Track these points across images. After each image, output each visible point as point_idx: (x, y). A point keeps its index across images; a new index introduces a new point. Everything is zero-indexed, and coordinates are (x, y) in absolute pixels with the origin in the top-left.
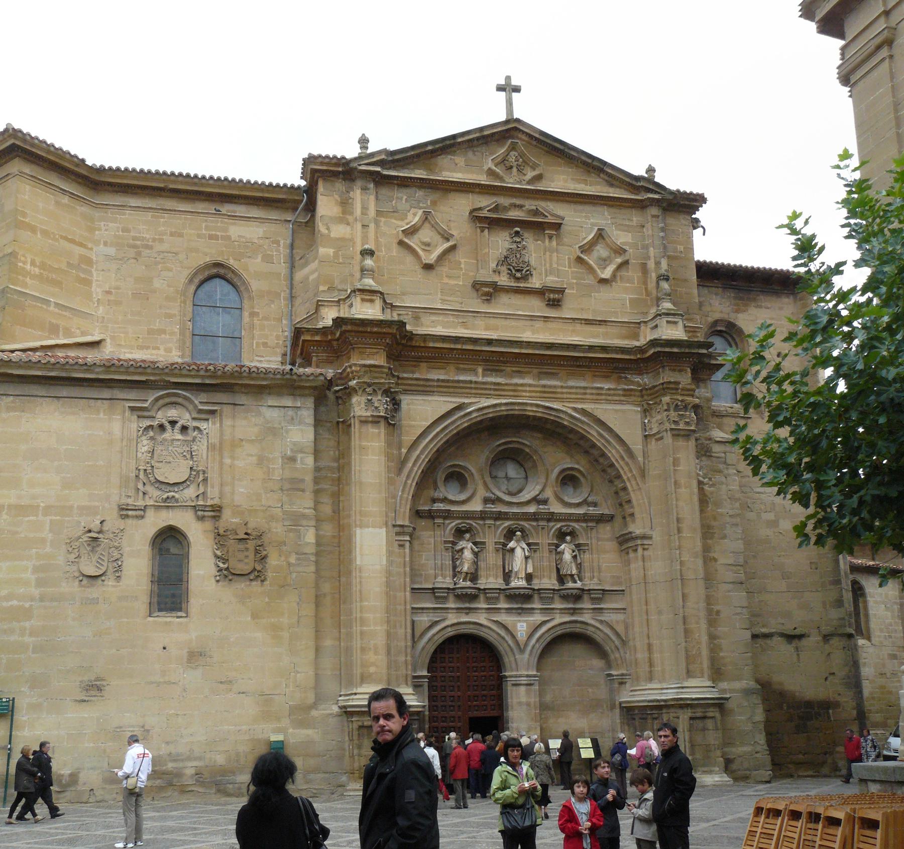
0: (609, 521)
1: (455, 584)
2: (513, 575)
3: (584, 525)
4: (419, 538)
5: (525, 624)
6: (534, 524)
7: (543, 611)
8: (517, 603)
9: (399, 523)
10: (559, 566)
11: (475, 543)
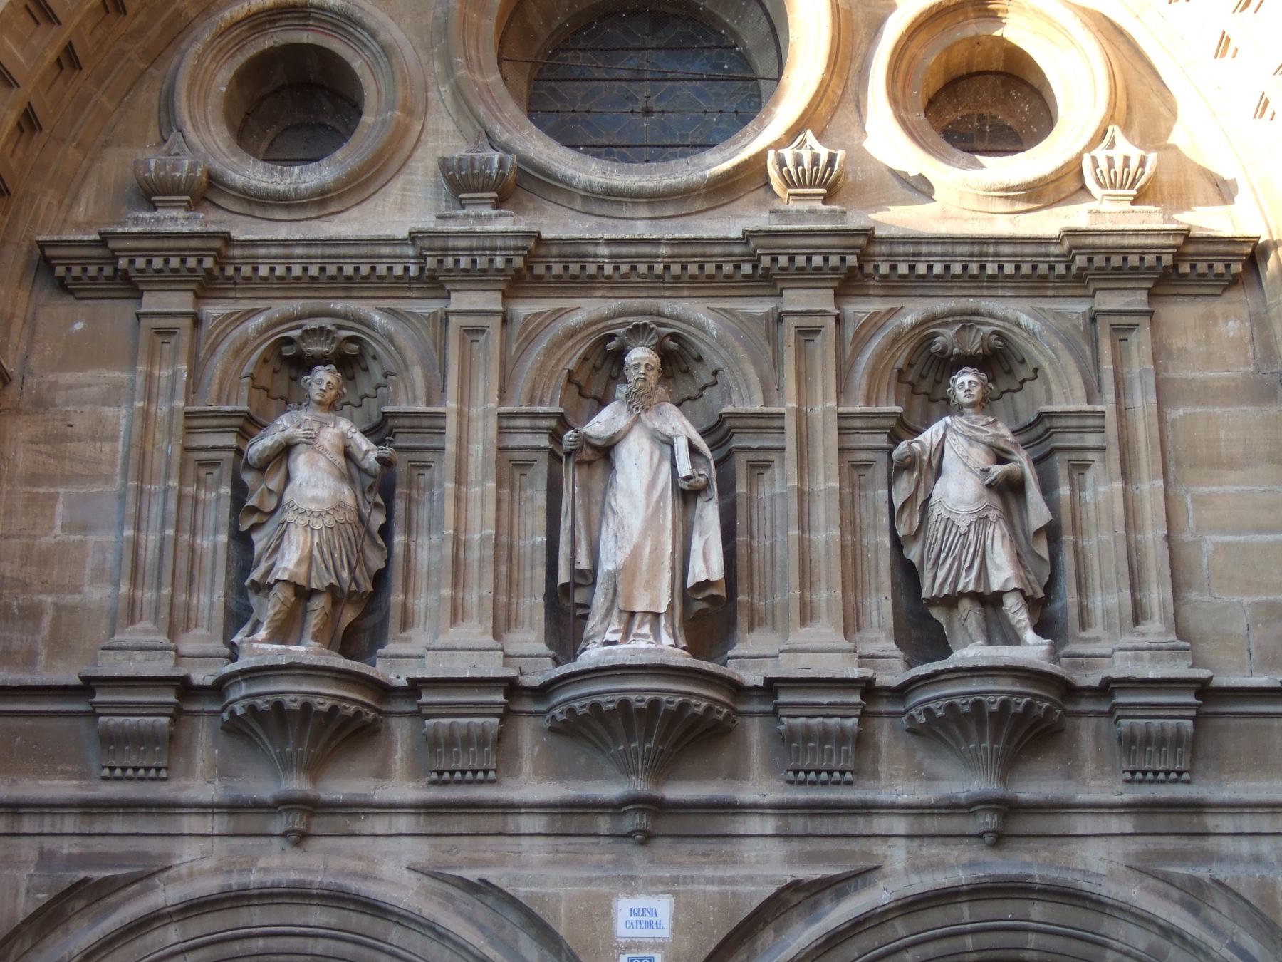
0: (1234, 282)
1: (233, 658)
2: (599, 600)
3: (1077, 308)
4: (41, 404)
5: (663, 907)
6: (760, 307)
7: (798, 825)
8: (628, 770)
10: (913, 554)
11: (379, 430)
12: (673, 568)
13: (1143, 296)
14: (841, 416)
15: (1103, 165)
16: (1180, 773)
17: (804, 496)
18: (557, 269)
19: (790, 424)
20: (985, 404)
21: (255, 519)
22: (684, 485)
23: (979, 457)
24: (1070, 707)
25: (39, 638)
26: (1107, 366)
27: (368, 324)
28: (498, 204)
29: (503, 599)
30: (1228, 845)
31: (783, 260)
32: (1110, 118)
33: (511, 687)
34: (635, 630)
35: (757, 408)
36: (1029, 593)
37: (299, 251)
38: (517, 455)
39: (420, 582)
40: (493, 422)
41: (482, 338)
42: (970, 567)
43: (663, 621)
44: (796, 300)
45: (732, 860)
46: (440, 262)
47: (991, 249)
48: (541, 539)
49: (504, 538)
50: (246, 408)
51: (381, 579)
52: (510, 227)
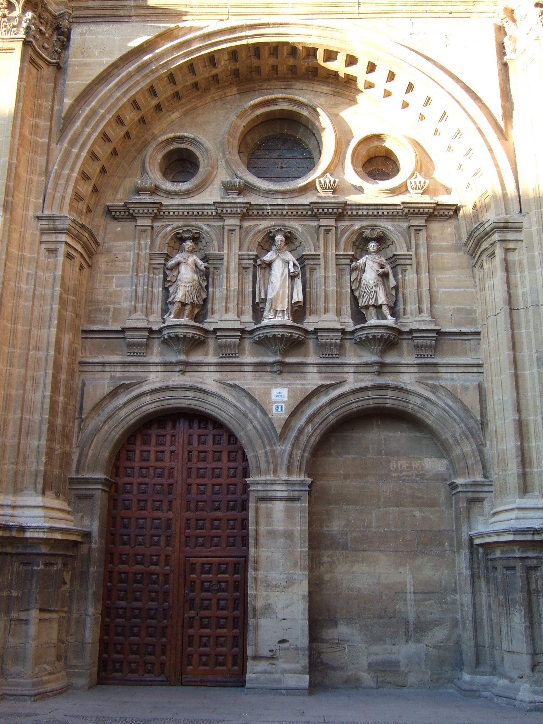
0: (450, 217)
1: (164, 323)
2: (267, 307)
3: (405, 224)
4: (109, 251)
5: (285, 391)
6: (314, 224)
7: (323, 369)
8: (275, 354)
9: (47, 212)
10: (357, 294)
11: (205, 259)
12: (288, 298)
13: (424, 221)
14: (336, 255)
15: (413, 183)
16: (431, 355)
17: (326, 278)
18: (255, 213)
19: (322, 257)
20: (378, 252)
21: (170, 284)
22: (292, 274)
23: (376, 267)
24: (400, 337)
25: (109, 317)
26: (413, 241)
27: (202, 229)
28: (238, 194)
29: (240, 306)
30: (444, 375)
31: (320, 211)
32: (416, 170)
33: (242, 331)
34: (277, 315)
35: (313, 253)
36: (389, 305)
37: (181, 208)
38: (244, 266)
39: (217, 302)
40: (237, 256)
41: (234, 233)
42: (373, 298)
43: (285, 313)
44: (324, 222)
45: (304, 379)
46: (222, 211)
47: (380, 207)
48: (251, 289)
49: (240, 289)
50: (167, 252)
51: (205, 300)
52: (242, 201)
